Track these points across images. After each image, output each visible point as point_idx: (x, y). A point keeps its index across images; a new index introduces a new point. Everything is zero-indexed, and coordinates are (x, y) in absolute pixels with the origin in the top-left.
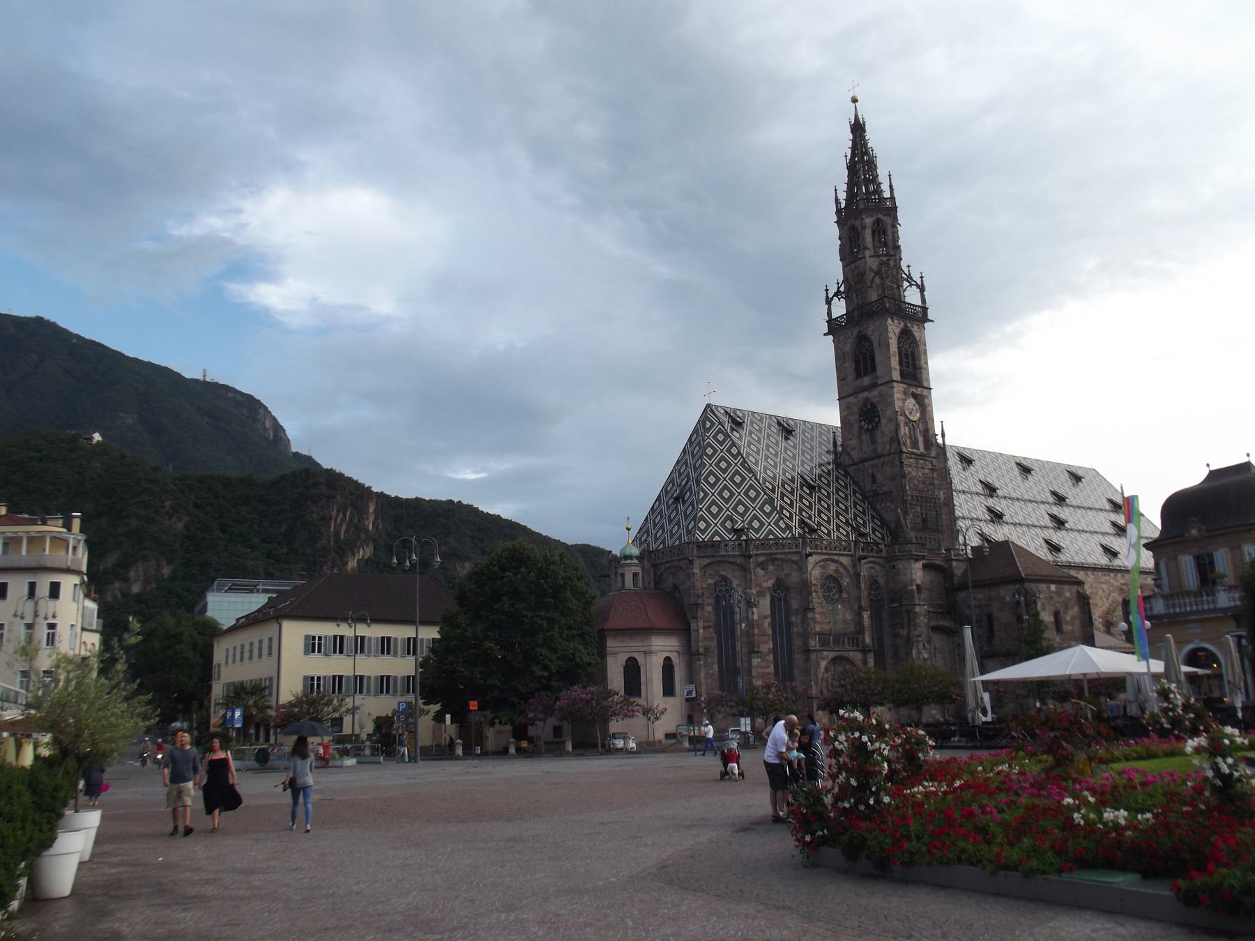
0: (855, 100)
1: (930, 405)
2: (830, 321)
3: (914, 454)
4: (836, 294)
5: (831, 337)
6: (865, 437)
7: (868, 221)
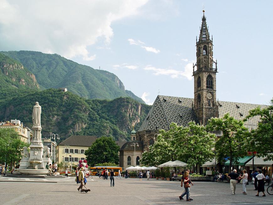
0: (204, 11)
1: (215, 95)
2: (194, 72)
3: (208, 108)
4: (196, 65)
5: (194, 77)
6: (198, 103)
7: (203, 46)
